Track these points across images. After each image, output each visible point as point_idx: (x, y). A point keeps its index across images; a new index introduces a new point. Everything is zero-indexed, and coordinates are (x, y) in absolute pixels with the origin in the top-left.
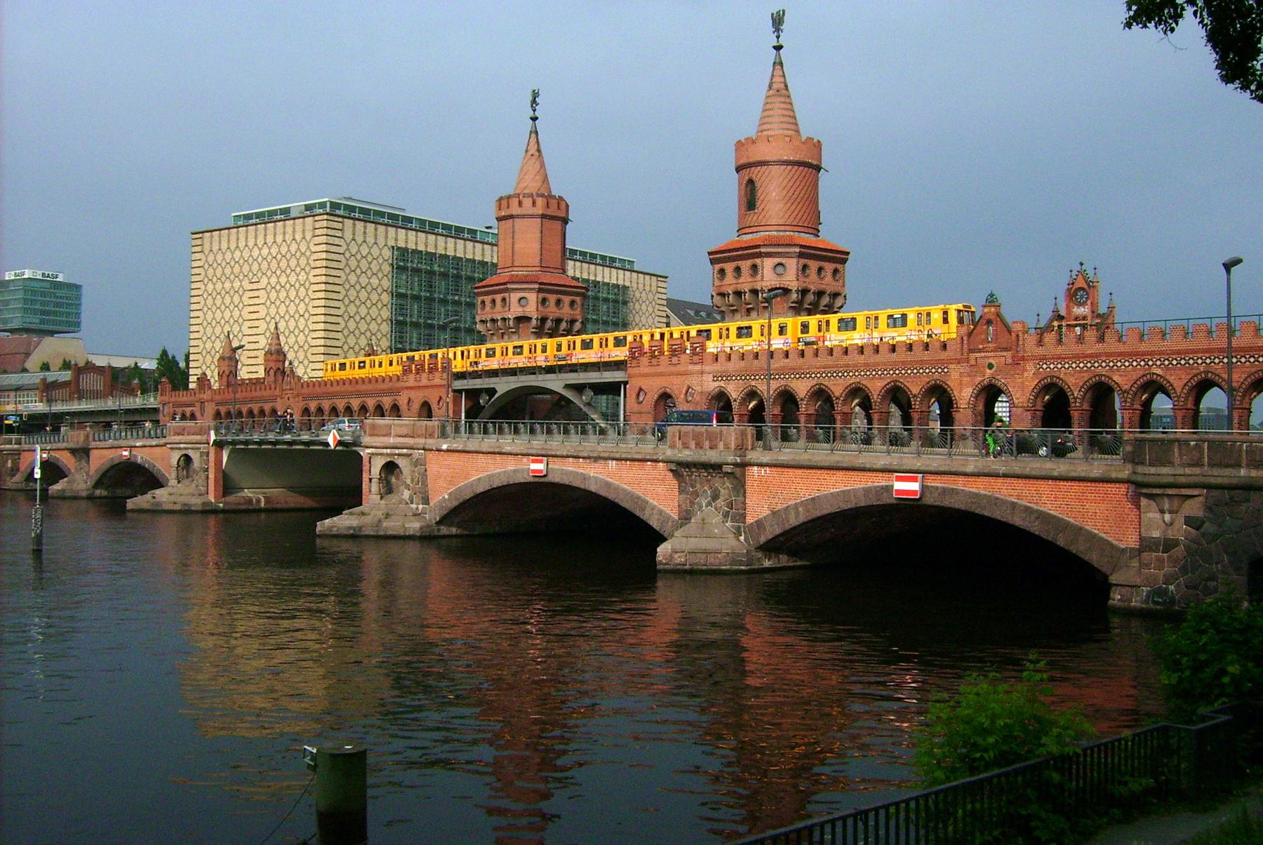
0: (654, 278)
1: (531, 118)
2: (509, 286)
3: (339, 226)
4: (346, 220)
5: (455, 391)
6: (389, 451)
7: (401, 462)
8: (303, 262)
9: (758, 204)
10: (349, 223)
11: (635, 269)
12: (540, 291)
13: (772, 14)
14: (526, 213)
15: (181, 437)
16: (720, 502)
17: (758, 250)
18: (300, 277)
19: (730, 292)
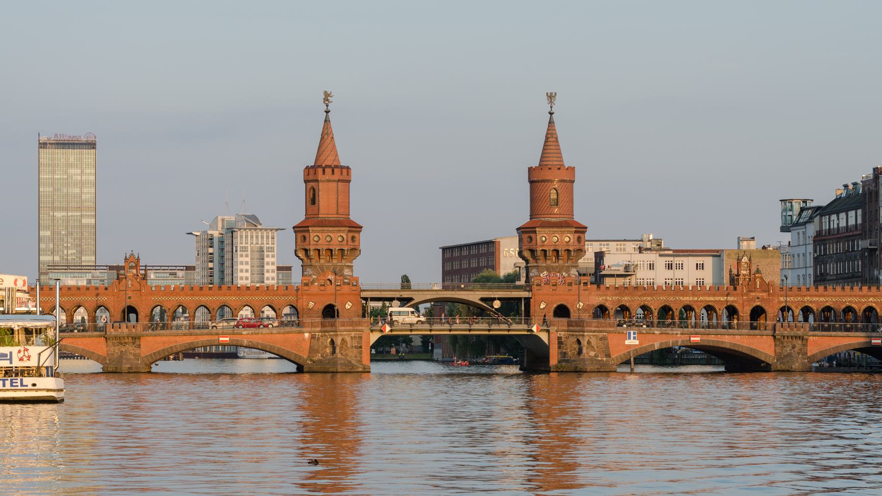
5: (361, 297)
13: (547, 93)
14: (344, 179)
16: (796, 349)
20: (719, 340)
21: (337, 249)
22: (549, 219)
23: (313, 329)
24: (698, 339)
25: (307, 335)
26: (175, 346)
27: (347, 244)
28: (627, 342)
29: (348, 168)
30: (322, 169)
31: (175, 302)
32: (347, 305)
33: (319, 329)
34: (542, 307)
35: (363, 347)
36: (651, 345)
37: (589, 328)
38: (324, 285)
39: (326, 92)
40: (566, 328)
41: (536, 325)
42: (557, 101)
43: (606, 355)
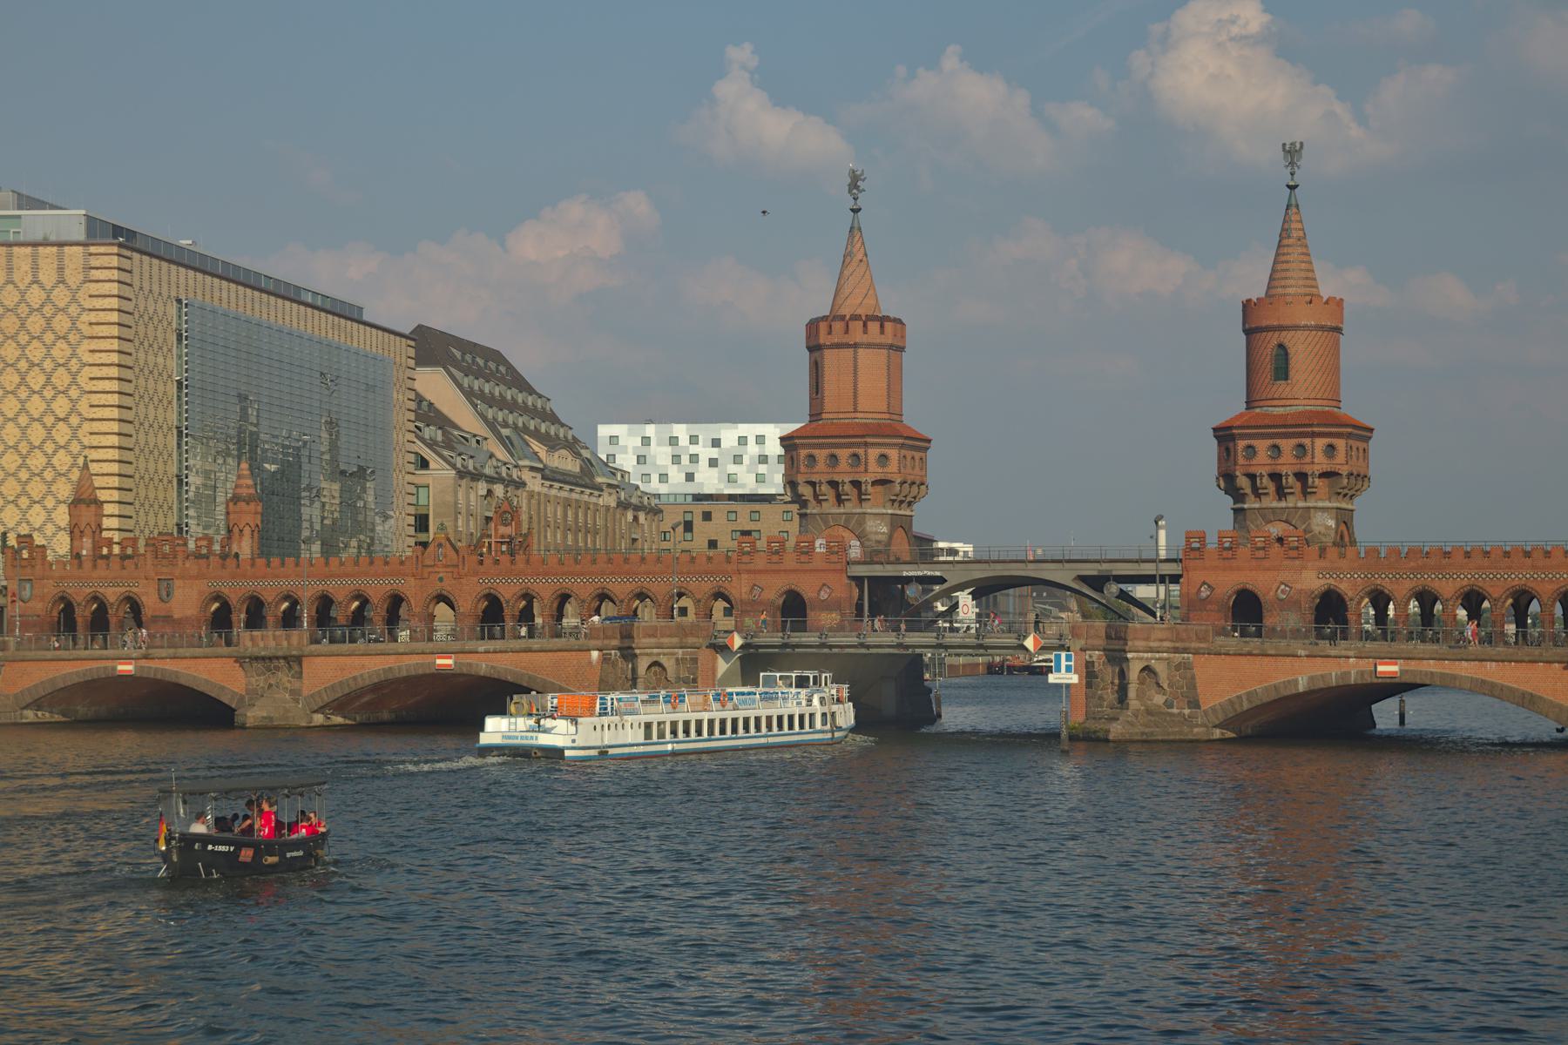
0: (404, 340)
1: (852, 210)
2: (869, 440)
3: (126, 264)
4: (134, 254)
5: (849, 577)
6: (1150, 655)
7: (1160, 668)
8: (61, 324)
9: (1292, 373)
10: (136, 256)
11: (366, 318)
12: (902, 446)
13: (1284, 145)
15: (653, 640)
17: (1310, 430)
18: (55, 352)
19: (1264, 473)
20: (1447, 671)
21: (847, 480)
22: (1270, 409)
23: (606, 642)
24: (1395, 668)
25: (595, 654)
26: (361, 675)
27: (866, 471)
28: (1052, 678)
29: (898, 321)
30: (861, 323)
31: (518, 588)
32: (822, 593)
33: (615, 642)
34: (1204, 595)
35: (699, 680)
36: (1289, 681)
37: (1140, 644)
38: (807, 553)
39: (853, 172)
40: (1101, 642)
41: (1032, 636)
42: (1305, 161)
43: (1189, 702)
